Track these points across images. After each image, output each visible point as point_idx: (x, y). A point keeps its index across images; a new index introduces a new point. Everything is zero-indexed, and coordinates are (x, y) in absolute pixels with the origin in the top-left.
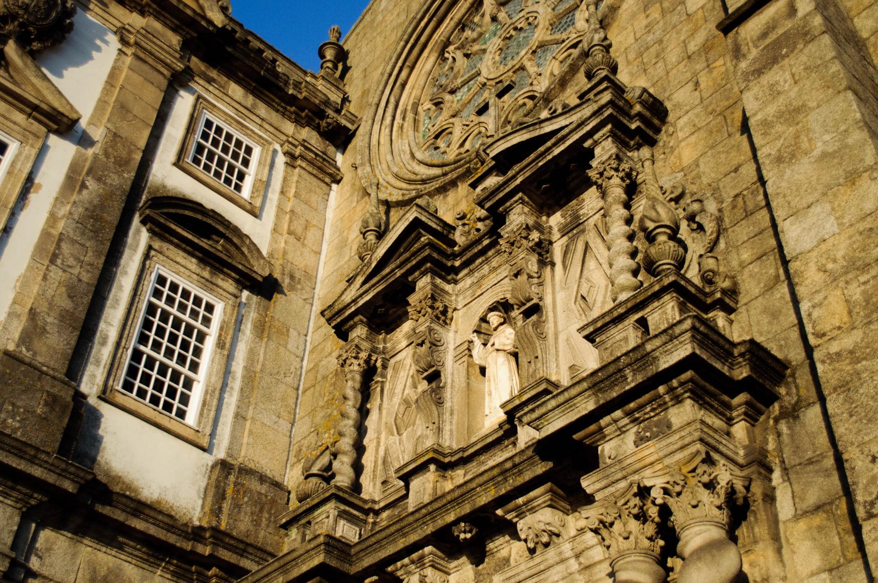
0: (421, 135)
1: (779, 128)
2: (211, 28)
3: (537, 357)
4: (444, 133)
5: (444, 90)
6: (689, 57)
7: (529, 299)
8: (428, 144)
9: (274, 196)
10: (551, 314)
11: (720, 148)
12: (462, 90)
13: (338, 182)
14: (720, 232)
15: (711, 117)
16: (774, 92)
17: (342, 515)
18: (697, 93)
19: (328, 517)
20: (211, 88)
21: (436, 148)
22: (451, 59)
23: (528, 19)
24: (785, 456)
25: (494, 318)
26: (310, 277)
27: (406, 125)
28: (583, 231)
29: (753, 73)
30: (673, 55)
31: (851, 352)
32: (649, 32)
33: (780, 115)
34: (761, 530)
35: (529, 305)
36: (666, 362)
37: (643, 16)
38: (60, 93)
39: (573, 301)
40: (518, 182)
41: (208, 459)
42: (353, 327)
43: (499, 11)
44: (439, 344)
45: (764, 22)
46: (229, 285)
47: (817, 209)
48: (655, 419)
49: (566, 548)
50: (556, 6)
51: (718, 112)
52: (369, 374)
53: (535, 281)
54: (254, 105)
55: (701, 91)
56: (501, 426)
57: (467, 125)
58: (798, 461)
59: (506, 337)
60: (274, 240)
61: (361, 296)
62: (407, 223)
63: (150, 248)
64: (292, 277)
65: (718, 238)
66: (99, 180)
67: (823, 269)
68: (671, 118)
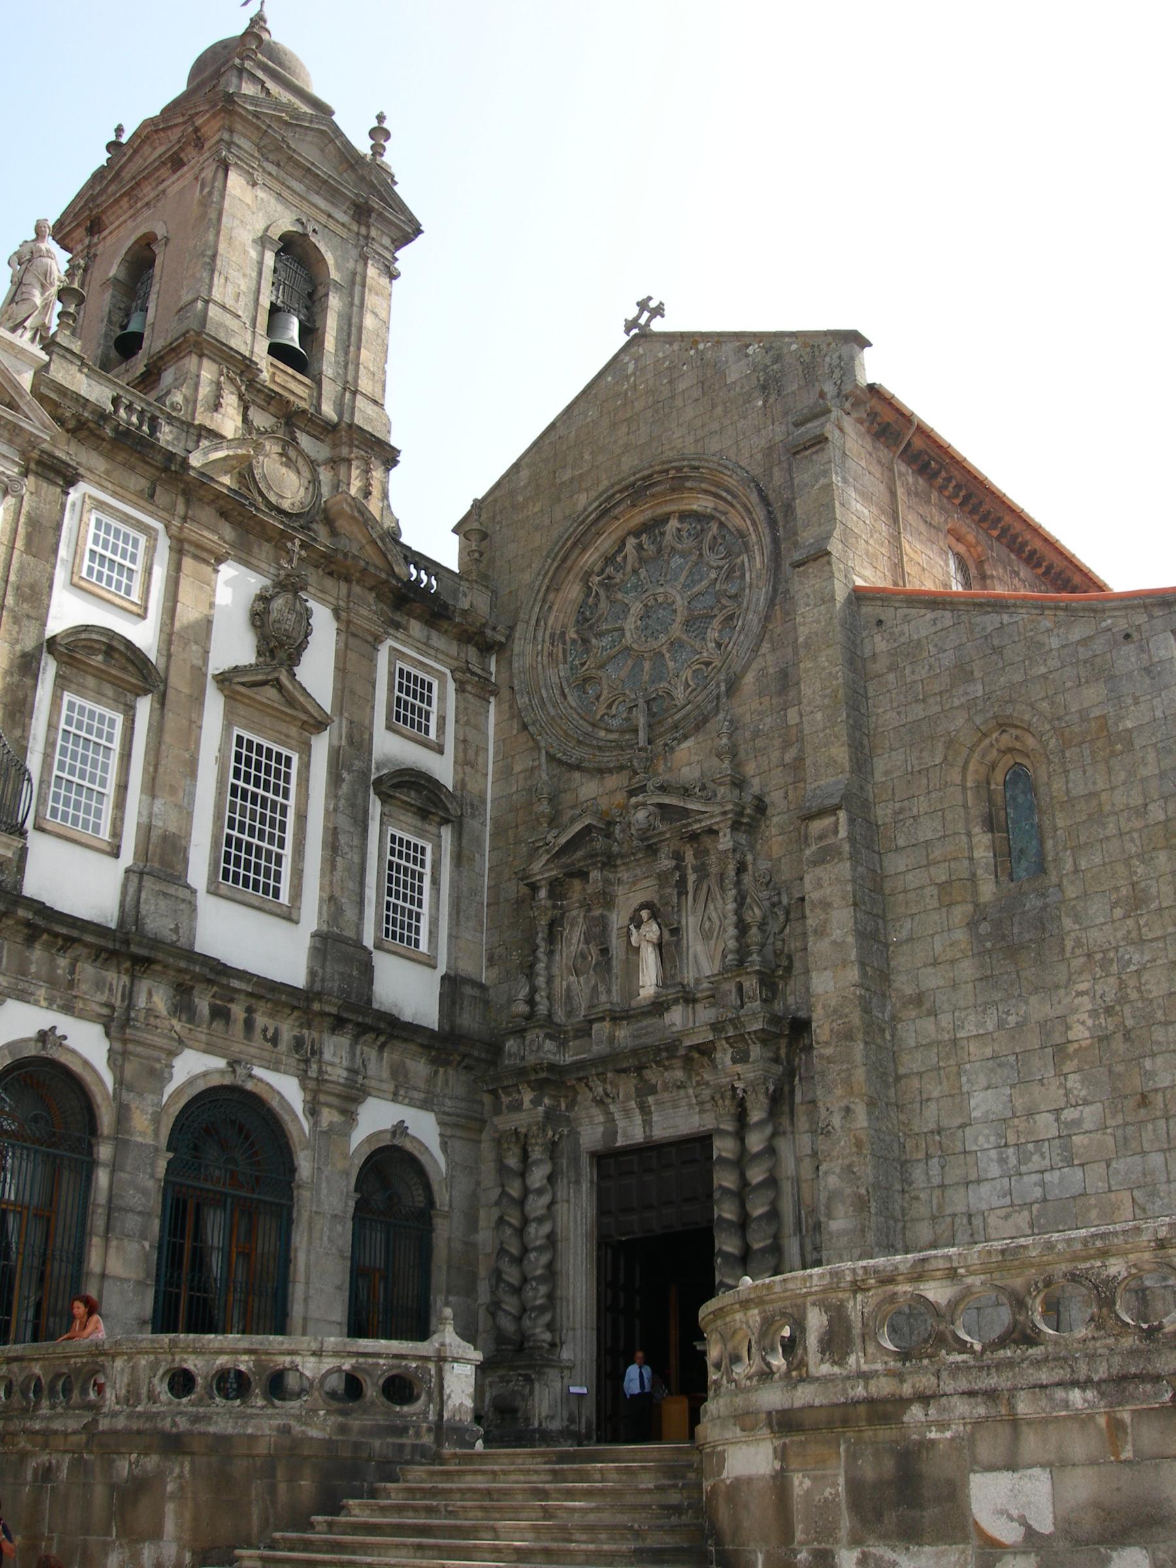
0: (567, 666)
1: (818, 910)
13: (496, 696)
16: (819, 885)
17: (548, 1036)
20: (398, 635)
25: (645, 914)
26: (484, 802)
28: (708, 876)
30: (775, 755)
32: (761, 720)
34: (786, 1109)
38: (304, 689)
46: (432, 829)
49: (691, 1091)
54: (429, 638)
56: (653, 1004)
59: (651, 930)
61: (548, 870)
63: (383, 814)
64: (472, 805)
65: (785, 927)
66: (350, 771)
67: (824, 1007)
68: (769, 812)
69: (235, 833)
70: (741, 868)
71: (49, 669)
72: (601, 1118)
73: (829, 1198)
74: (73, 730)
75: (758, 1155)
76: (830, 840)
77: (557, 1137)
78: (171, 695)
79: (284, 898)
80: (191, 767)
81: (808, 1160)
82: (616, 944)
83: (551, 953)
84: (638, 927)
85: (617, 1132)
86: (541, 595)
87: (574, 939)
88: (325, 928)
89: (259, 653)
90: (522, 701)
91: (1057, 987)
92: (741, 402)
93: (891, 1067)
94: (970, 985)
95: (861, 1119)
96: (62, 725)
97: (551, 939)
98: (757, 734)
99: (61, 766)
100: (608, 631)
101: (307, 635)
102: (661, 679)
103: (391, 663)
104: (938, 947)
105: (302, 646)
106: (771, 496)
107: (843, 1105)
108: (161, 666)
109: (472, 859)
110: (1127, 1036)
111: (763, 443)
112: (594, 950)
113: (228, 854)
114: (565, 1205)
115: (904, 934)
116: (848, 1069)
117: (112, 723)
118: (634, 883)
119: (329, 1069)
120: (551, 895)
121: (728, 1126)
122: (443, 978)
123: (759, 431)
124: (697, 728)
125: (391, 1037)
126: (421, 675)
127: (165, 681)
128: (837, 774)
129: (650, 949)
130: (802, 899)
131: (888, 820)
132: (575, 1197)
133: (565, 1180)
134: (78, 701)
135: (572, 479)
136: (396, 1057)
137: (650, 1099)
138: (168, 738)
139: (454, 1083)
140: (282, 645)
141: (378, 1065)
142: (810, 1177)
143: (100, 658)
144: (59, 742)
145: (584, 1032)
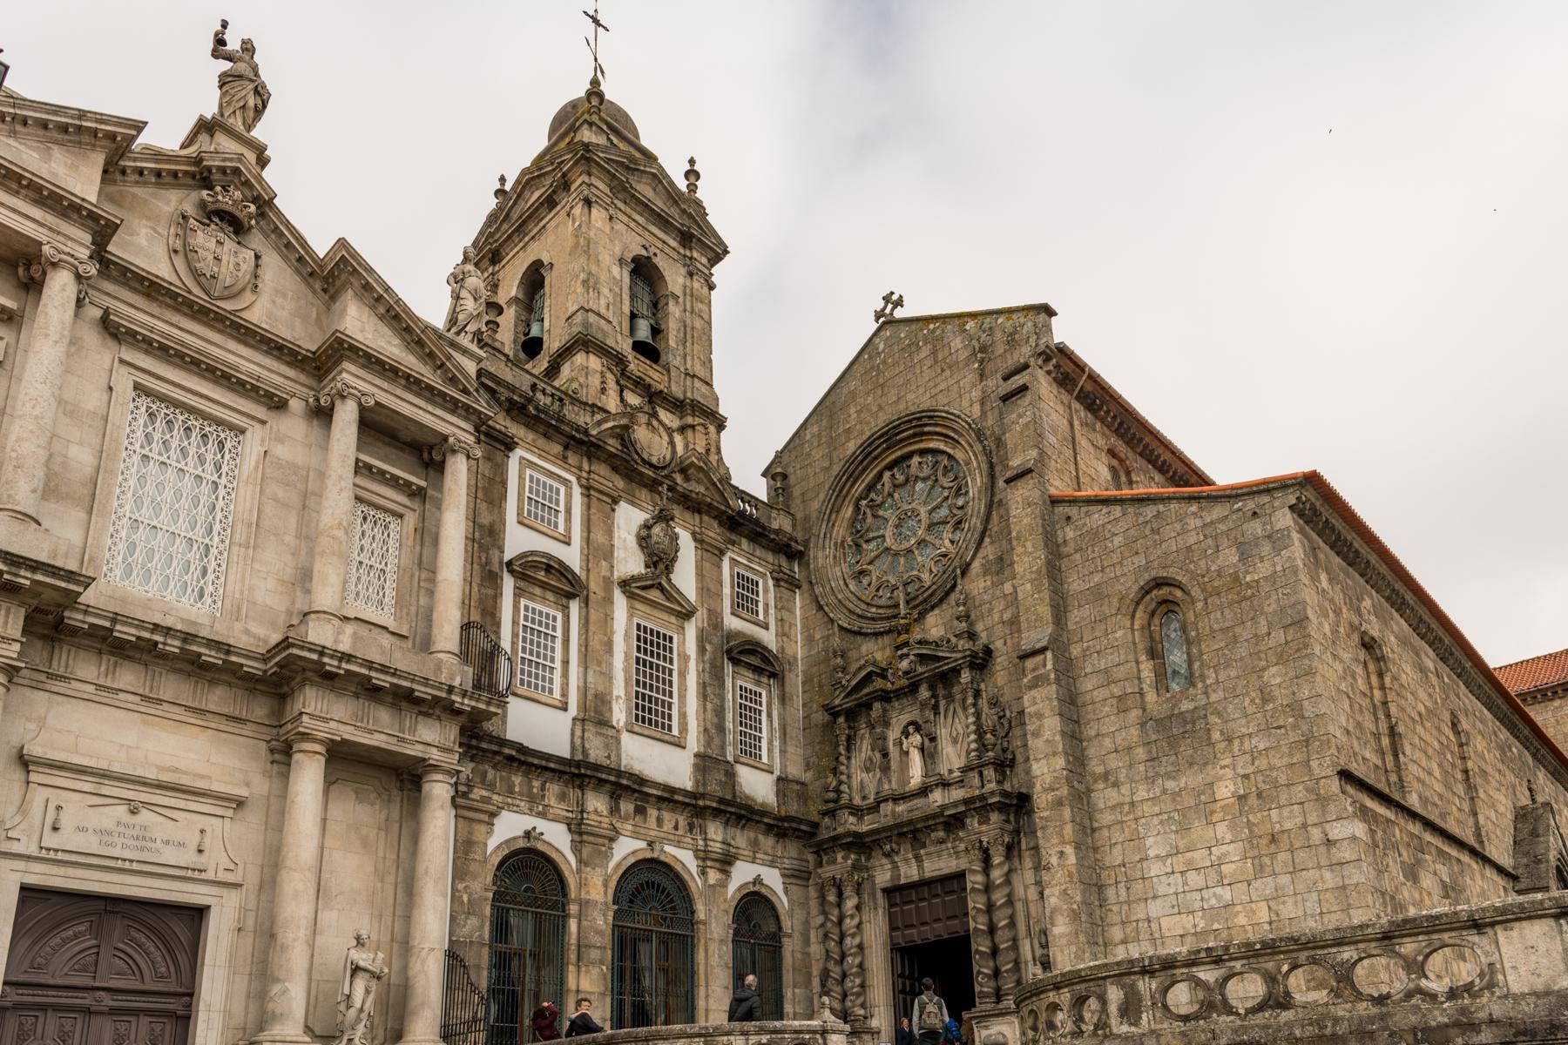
1: (1034, 719)
9: (772, 611)
14: (1010, 728)
17: (851, 814)
25: (911, 729)
26: (796, 659)
30: (996, 617)
41: (775, 777)
46: (765, 680)
59: (916, 739)
63: (734, 672)
69: (641, 690)
70: (977, 694)
71: (508, 584)
74: (529, 624)
78: (592, 596)
79: (675, 732)
80: (609, 646)
82: (893, 751)
83: (849, 758)
84: (907, 738)
87: (864, 749)
88: (702, 750)
89: (647, 566)
90: (819, 589)
91: (1206, 763)
93: (1087, 822)
94: (1142, 768)
95: (1072, 859)
96: (522, 622)
97: (848, 749)
99: (524, 650)
100: (874, 538)
101: (677, 551)
102: (912, 569)
103: (731, 569)
104: (1119, 740)
105: (674, 560)
108: (583, 576)
109: (791, 699)
110: (1259, 795)
112: (878, 755)
113: (637, 704)
115: (1093, 733)
117: (555, 619)
118: (903, 709)
119: (711, 843)
120: (846, 721)
121: (977, 867)
122: (779, 779)
124: (941, 601)
125: (749, 820)
126: (751, 576)
127: (587, 588)
129: (916, 752)
130: (1021, 713)
134: (531, 605)
136: (752, 834)
138: (592, 628)
139: (791, 851)
140: (661, 559)
141: (741, 839)
143: (543, 573)
144: (521, 634)
145: (874, 808)
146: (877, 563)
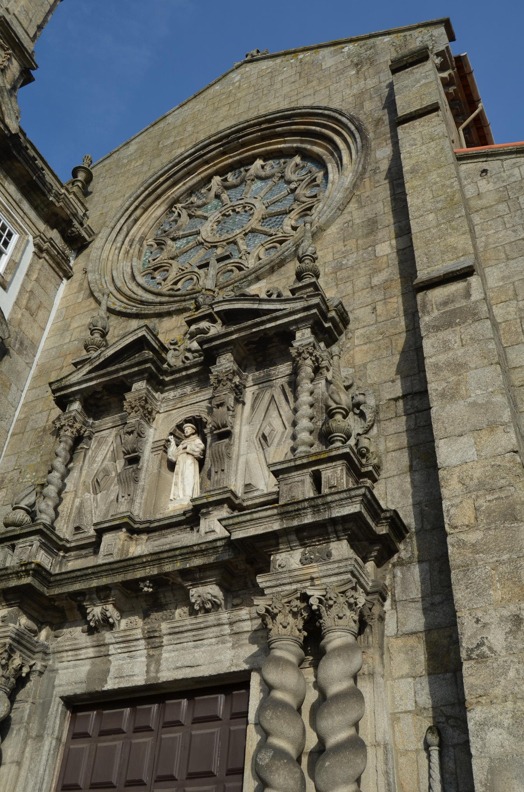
0: (141, 263)
1: (446, 373)
2: (6, 132)
3: (223, 470)
4: (162, 269)
5: (167, 236)
6: (372, 288)
7: (225, 426)
8: (147, 272)
10: (237, 441)
11: (384, 361)
12: (181, 240)
13: (68, 278)
15: (381, 337)
16: (446, 347)
17: (43, 546)
18: (374, 315)
19: (31, 545)
21: (153, 278)
22: (176, 214)
23: (244, 207)
24: (396, 592)
25: (189, 428)
26: (34, 347)
27: (131, 251)
28: (271, 387)
29: (433, 327)
30: (361, 281)
31: (473, 545)
32: (345, 257)
33: (448, 364)
35: (223, 430)
36: (338, 512)
37: (341, 244)
39: (255, 435)
40: (234, 337)
42: (72, 402)
43: (223, 192)
44: (143, 436)
45: (446, 294)
47: (464, 439)
48: (319, 547)
50: (269, 206)
51: (387, 334)
52: (78, 440)
53: (231, 413)
55: (376, 316)
57: (183, 270)
58: (405, 598)
60: (14, 311)
62: (135, 337)
64: (22, 344)
67: (461, 481)
68: (350, 326)
72: (91, 652)
73: (492, 771)
75: (340, 696)
76: (462, 303)
77: (25, 670)
81: (409, 719)
85: (108, 671)
86: (129, 212)
92: (335, 75)
97: (73, 450)
98: (339, 267)
106: (362, 117)
107: (506, 613)
111: (355, 91)
114: (14, 768)
116: (510, 560)
123: (351, 86)
128: (458, 257)
131: (510, 317)
132: (32, 759)
133: (22, 732)
135: (173, 143)
137: (165, 627)
142: (412, 747)
146: (181, 259)
